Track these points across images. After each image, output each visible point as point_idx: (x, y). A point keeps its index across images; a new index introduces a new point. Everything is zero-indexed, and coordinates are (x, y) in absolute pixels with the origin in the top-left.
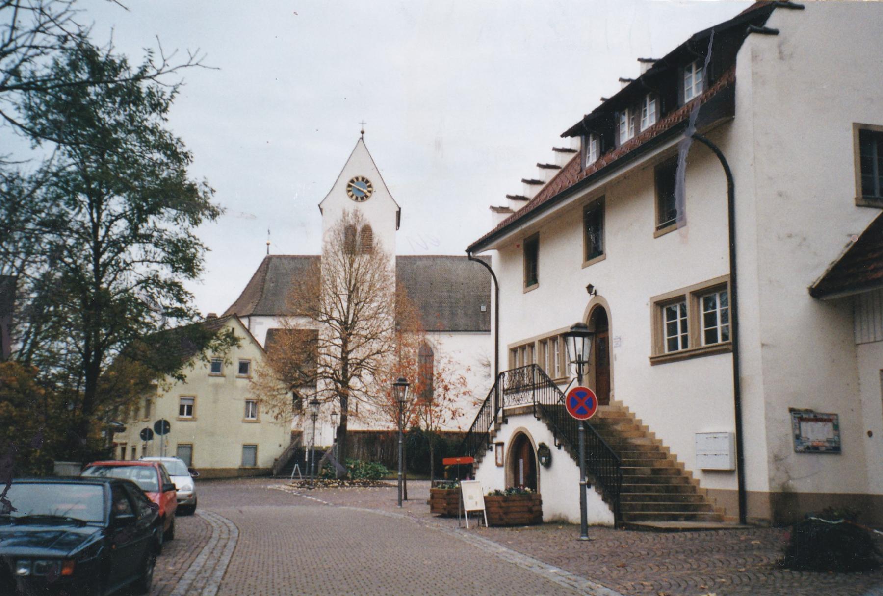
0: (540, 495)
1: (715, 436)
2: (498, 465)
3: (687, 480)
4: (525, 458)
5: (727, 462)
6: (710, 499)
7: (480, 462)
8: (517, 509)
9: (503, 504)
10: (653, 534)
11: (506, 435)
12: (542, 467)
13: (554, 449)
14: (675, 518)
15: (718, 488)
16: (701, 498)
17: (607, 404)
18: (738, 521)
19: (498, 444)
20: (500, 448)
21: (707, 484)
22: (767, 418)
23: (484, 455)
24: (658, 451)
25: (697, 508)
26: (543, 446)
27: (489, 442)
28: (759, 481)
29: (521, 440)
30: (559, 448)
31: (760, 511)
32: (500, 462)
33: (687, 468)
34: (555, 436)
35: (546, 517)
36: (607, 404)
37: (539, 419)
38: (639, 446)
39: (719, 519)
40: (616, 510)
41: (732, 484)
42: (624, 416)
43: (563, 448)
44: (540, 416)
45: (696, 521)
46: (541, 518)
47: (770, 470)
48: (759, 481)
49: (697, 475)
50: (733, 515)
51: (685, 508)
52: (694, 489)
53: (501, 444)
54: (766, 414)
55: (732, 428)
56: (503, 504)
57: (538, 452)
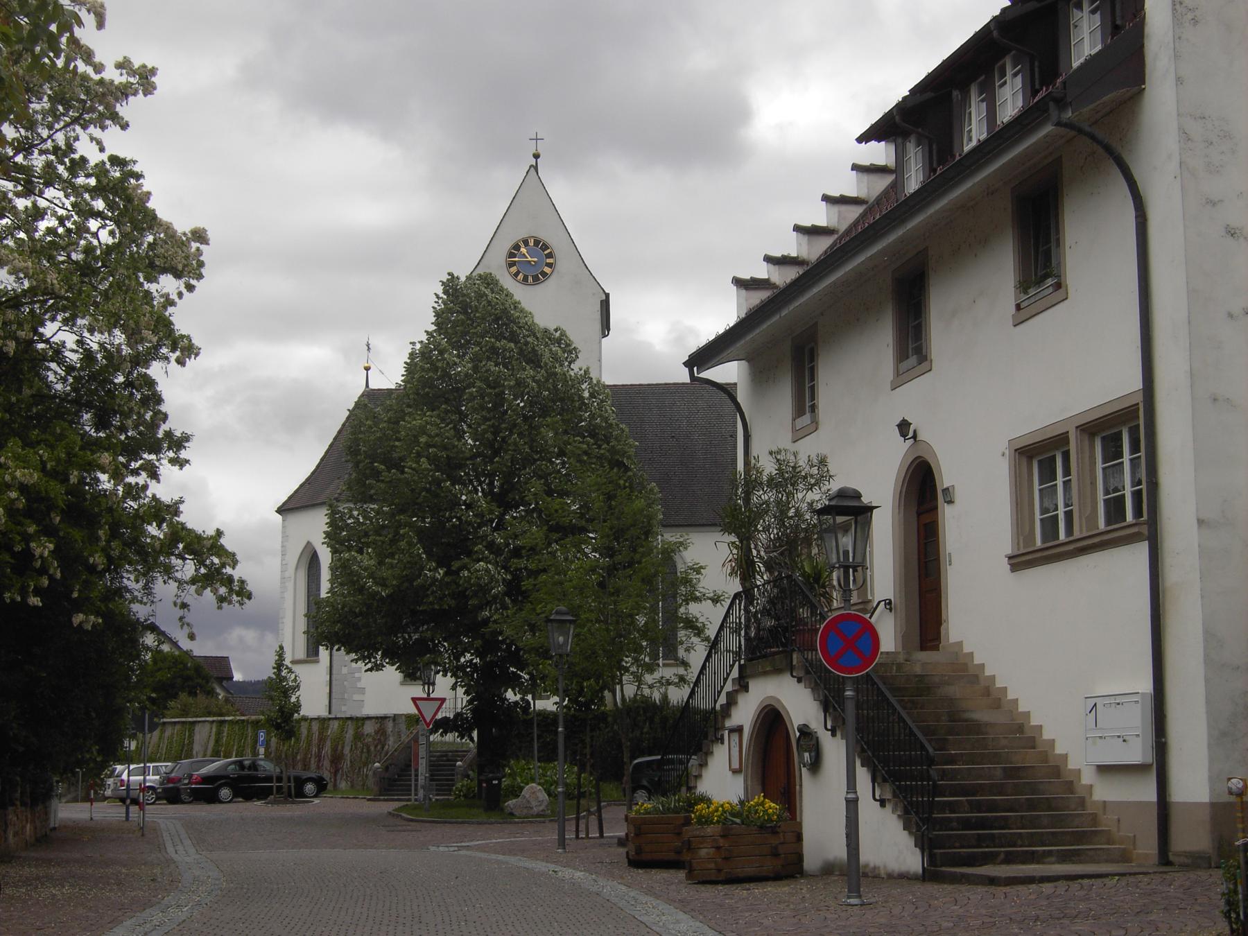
0: (800, 824)
1: (1117, 700)
2: (735, 772)
3: (1070, 786)
4: (777, 755)
5: (1137, 752)
6: (1108, 822)
7: (703, 765)
8: (764, 851)
9: (721, 842)
10: (981, 889)
11: (745, 714)
12: (804, 770)
13: (825, 738)
14: (1032, 858)
15: (1132, 799)
16: (1094, 819)
17: (936, 648)
18: (1155, 860)
19: (732, 731)
20: (735, 737)
21: (1105, 792)
22: (1208, 661)
23: (709, 753)
24: (1023, 733)
25: (1080, 837)
26: (805, 732)
27: (718, 728)
28: (1193, 783)
29: (772, 719)
30: (834, 735)
31: (1192, 837)
32: (736, 765)
33: (1072, 765)
34: (826, 710)
35: (811, 861)
36: (936, 648)
37: (799, 680)
38: (987, 724)
39: (1125, 857)
40: (925, 844)
41: (1146, 792)
42: (966, 671)
43: (839, 734)
44: (801, 674)
45: (1081, 862)
46: (802, 866)
47: (1212, 760)
48: (1193, 783)
49: (1088, 777)
50: (1148, 846)
51: (1055, 839)
52: (1082, 802)
53: (739, 730)
54: (1206, 656)
55: (1145, 685)
56: (721, 842)
57: (799, 740)
